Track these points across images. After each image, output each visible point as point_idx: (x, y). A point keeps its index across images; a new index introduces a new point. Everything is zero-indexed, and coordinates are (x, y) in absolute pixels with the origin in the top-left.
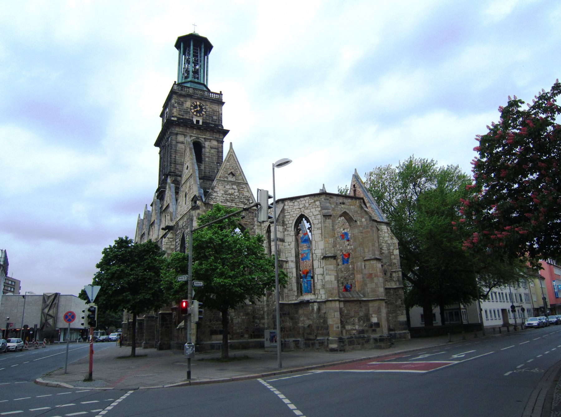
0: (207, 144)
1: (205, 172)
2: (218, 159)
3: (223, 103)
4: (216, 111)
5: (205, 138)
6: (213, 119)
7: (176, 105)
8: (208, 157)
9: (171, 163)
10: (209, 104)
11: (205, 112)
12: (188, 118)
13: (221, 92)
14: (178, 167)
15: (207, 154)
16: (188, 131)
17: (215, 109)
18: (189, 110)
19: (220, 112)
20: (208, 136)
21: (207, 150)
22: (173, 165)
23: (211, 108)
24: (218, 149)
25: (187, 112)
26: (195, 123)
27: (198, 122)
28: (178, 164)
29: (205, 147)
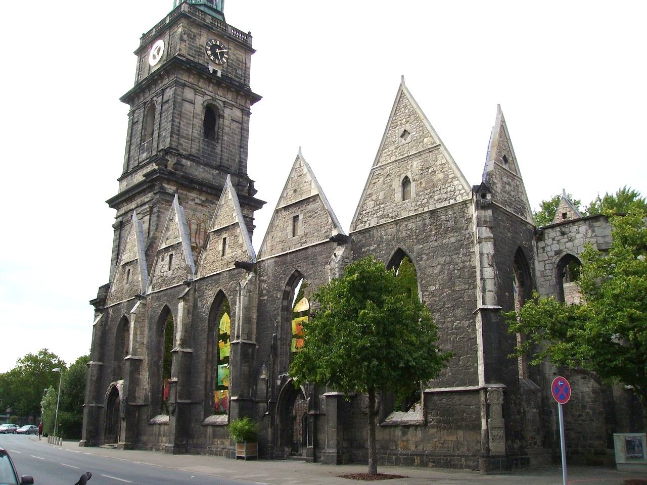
0: (227, 112)
1: (221, 159)
3: (253, 51)
4: (242, 62)
5: (224, 102)
6: (237, 73)
7: (185, 37)
8: (228, 134)
9: (172, 132)
10: (232, 48)
11: (227, 59)
12: (201, 62)
13: (250, 33)
14: (182, 141)
15: (227, 130)
16: (201, 84)
17: (240, 57)
18: (203, 50)
19: (247, 66)
20: (230, 97)
22: (175, 136)
23: (235, 55)
24: (241, 124)
25: (200, 53)
26: (211, 72)
27: (215, 72)
28: (183, 137)
29: (223, 117)
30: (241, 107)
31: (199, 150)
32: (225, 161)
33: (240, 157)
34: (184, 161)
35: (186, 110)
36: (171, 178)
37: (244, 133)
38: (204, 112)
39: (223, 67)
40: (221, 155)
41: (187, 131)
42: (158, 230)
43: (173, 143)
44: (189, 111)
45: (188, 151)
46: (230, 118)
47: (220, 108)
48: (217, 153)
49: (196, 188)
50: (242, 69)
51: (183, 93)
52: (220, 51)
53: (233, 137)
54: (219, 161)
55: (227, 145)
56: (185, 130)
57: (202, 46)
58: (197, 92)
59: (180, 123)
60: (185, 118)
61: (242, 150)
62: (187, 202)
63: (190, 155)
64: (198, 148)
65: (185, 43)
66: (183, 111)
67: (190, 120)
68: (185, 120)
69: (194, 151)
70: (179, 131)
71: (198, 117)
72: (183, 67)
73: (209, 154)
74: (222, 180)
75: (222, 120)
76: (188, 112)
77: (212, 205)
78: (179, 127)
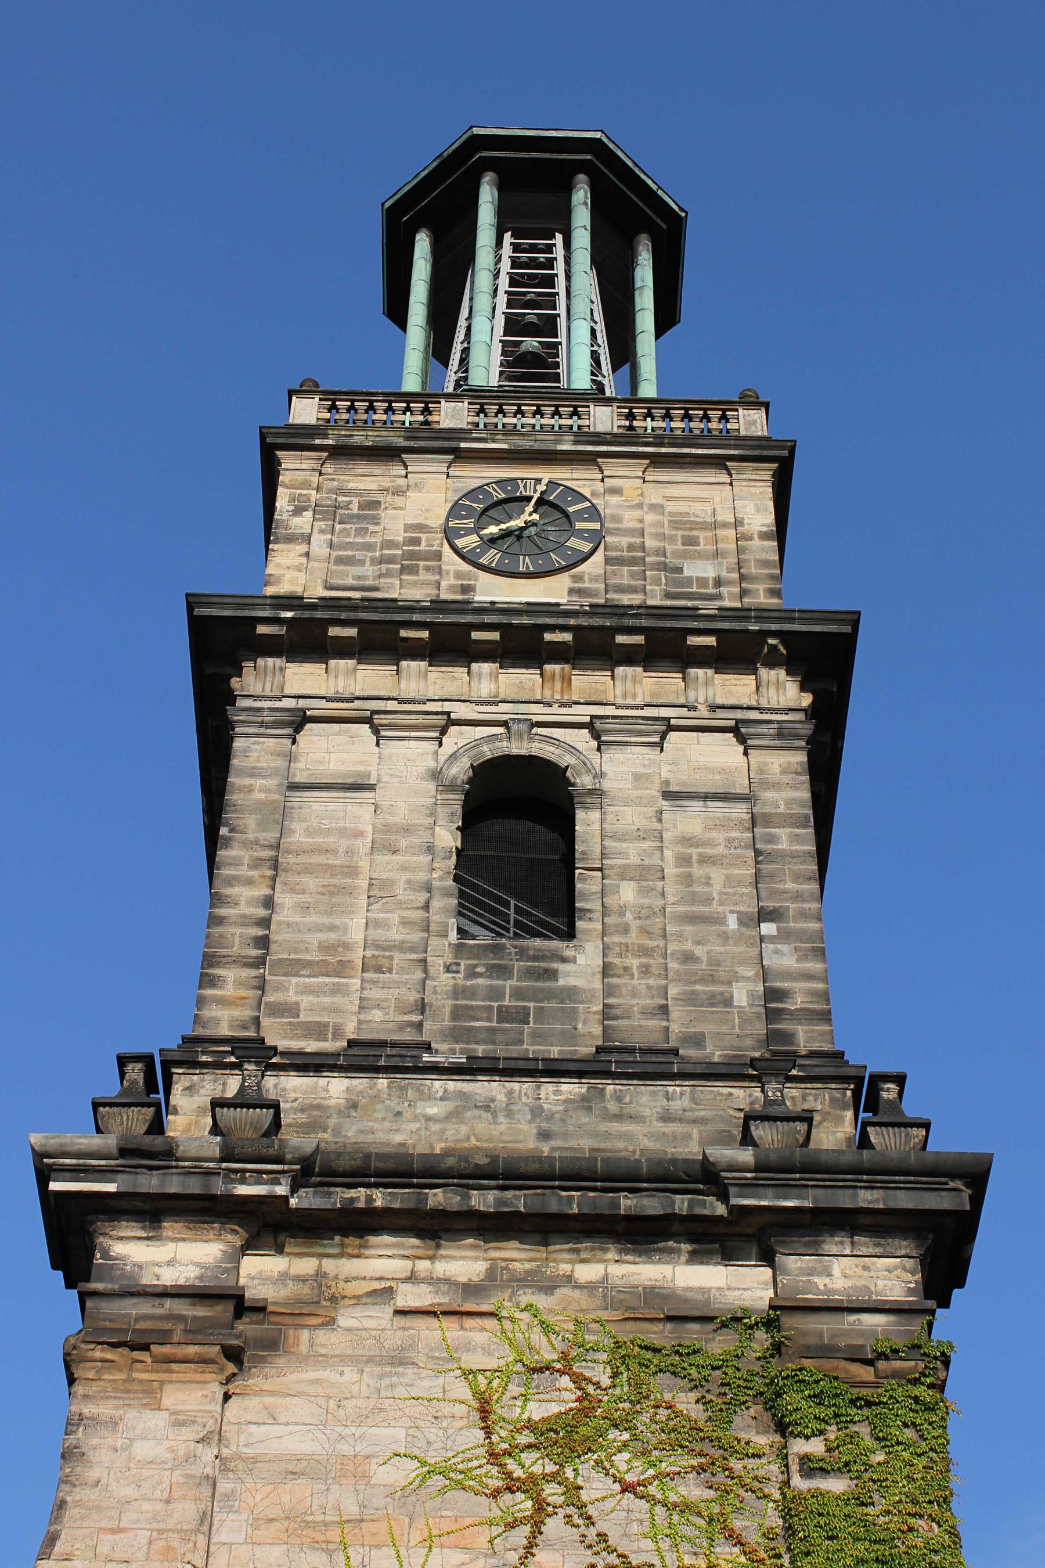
2: (757, 875)
4: (715, 525)
14: (290, 990)
17: (696, 508)
21: (630, 817)
25: (411, 559)
28: (294, 967)
30: (727, 718)
31: (422, 1007)
33: (765, 974)
34: (290, 1088)
35: (309, 832)
36: (150, 1183)
37: (771, 839)
38: (458, 809)
39: (577, 578)
41: (332, 928)
42: (59, 1548)
43: (211, 1012)
44: (343, 832)
45: (337, 1033)
46: (655, 791)
47: (566, 760)
48: (571, 993)
49: (370, 1212)
50: (717, 554)
51: (291, 758)
52: (530, 508)
53: (688, 879)
54: (597, 1030)
55: (644, 931)
56: (319, 929)
57: (420, 528)
58: (391, 726)
59: (269, 903)
60: (307, 870)
61: (768, 928)
62: (332, 1321)
63: (351, 1043)
64: (413, 996)
65: (303, 548)
66: (298, 836)
67: (352, 871)
68: (311, 883)
69: (382, 1021)
70: (263, 942)
71: (404, 843)
72: (262, 629)
73: (505, 1014)
74: (615, 1127)
75: (595, 815)
76: (331, 840)
77: (542, 1301)
78: (265, 923)
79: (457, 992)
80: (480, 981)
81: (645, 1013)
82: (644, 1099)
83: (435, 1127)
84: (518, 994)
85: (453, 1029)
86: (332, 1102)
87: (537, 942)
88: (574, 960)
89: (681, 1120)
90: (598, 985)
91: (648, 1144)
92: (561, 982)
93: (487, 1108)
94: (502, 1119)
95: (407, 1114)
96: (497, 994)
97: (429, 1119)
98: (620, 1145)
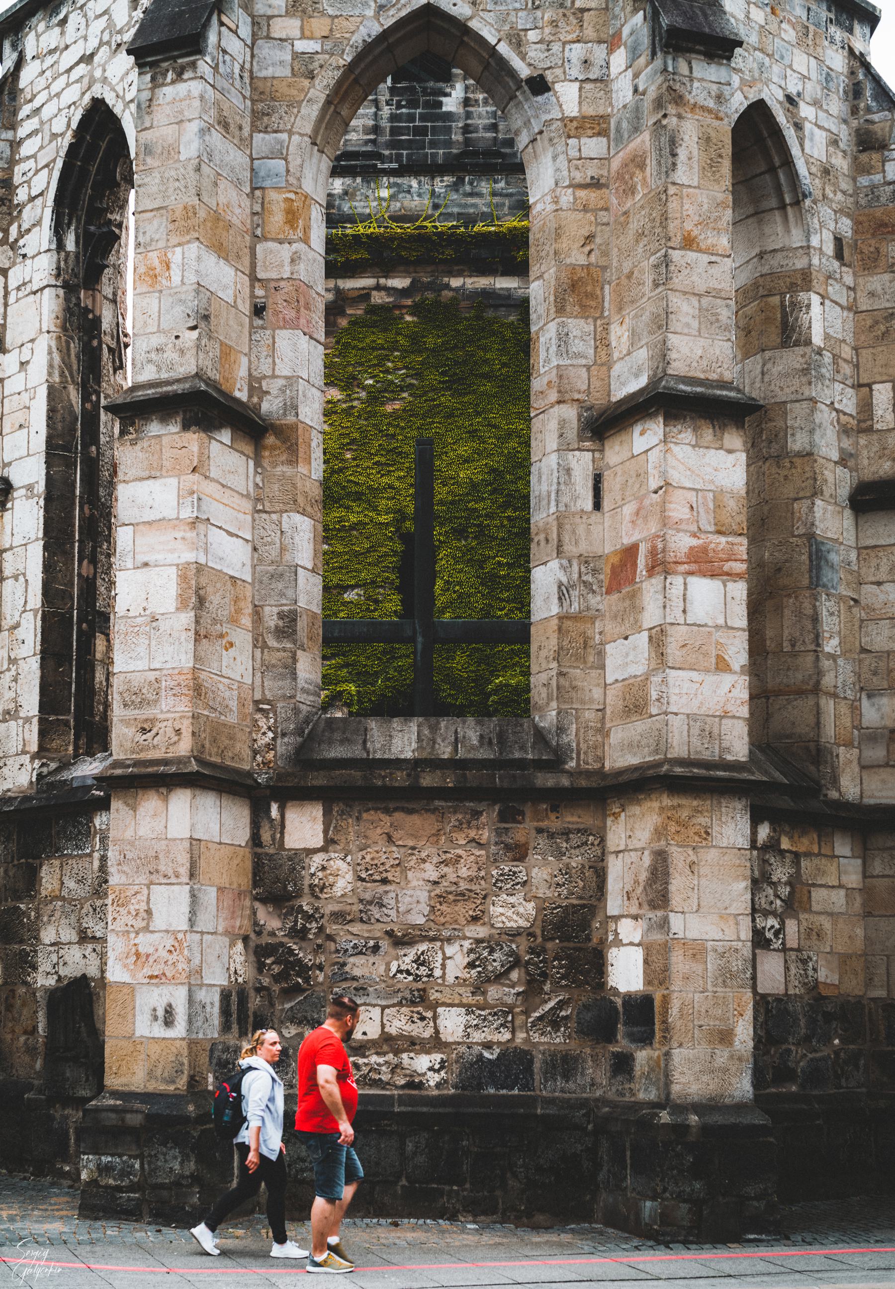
32: (482, 134)
40: (468, 115)
48: (449, 116)
64: (371, 123)
73: (418, 131)
74: (471, 201)
79: (393, 118)
80: (404, 110)
81: (487, 128)
82: (483, 184)
83: (384, 204)
84: (423, 118)
85: (391, 141)
86: (335, 192)
87: (431, 84)
88: (448, 95)
89: (501, 195)
90: (461, 110)
91: (485, 209)
92: (444, 109)
93: (409, 192)
94: (416, 198)
95: (371, 197)
96: (411, 118)
97: (381, 199)
98: (472, 211)
